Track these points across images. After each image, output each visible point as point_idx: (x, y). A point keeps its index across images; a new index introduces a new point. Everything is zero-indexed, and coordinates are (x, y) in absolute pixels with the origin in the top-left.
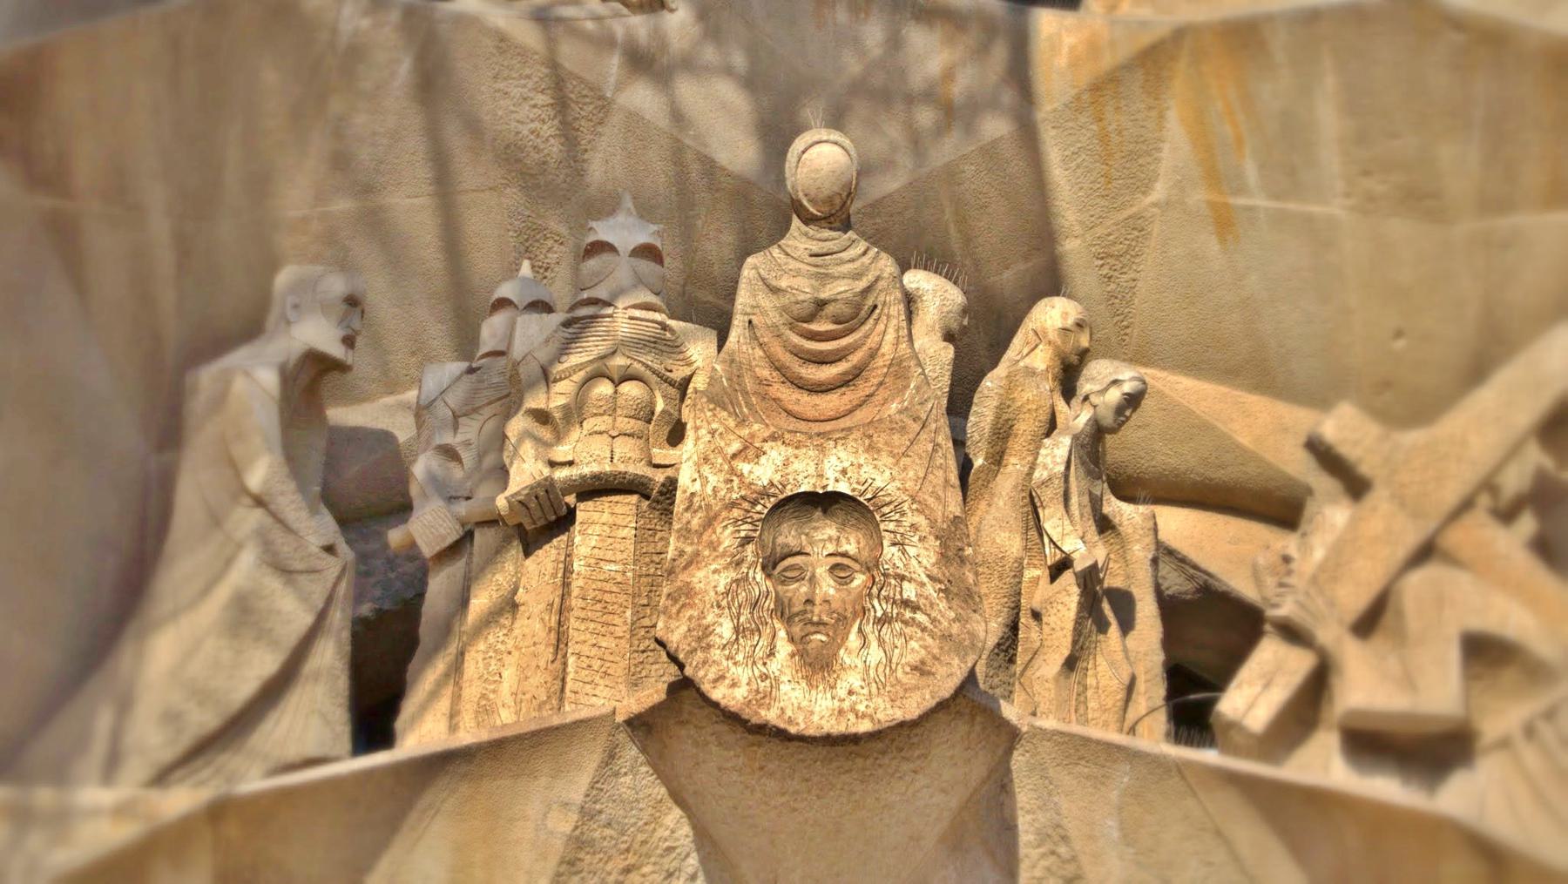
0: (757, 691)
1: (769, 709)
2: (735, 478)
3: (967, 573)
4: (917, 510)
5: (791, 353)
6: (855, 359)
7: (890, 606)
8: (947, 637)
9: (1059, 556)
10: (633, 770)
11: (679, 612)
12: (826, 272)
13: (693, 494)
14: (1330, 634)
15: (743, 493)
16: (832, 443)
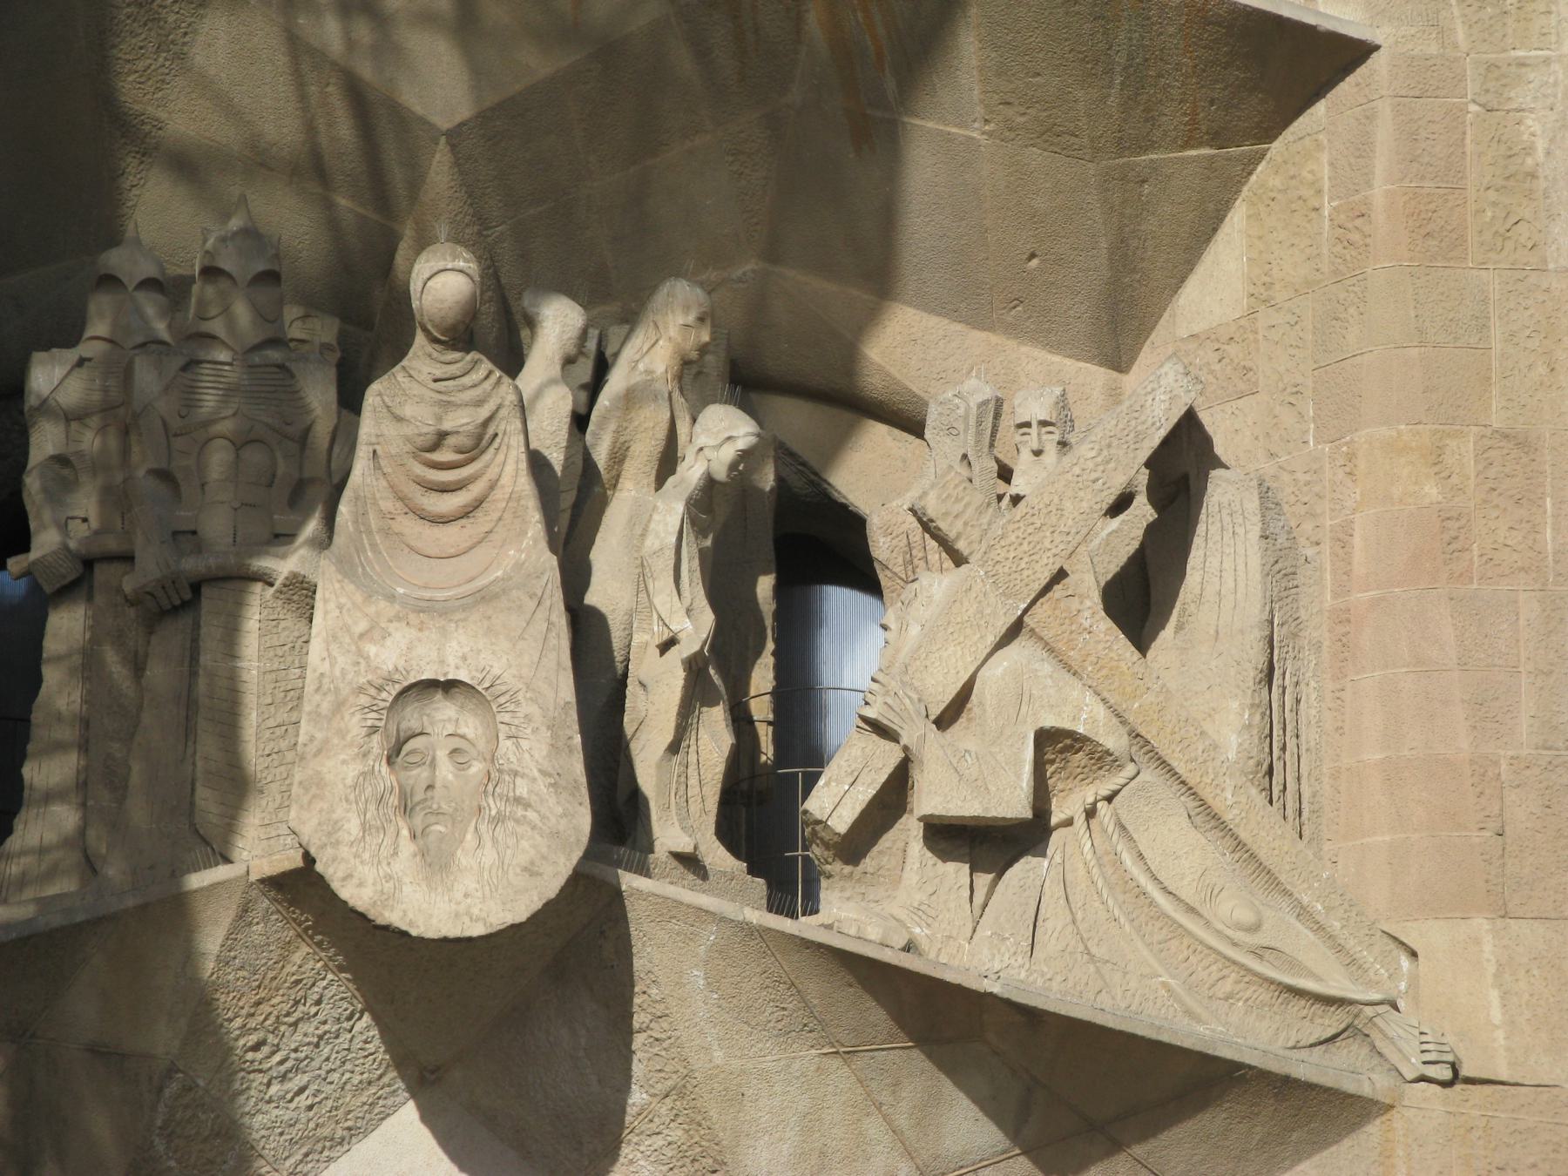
0: (382, 892)
1: (392, 911)
2: (361, 660)
3: (575, 763)
4: (531, 699)
5: (414, 482)
6: (476, 490)
7: (503, 804)
8: (555, 834)
9: (665, 637)
10: (265, 919)
11: (310, 802)
12: (449, 399)
13: (322, 674)
14: (915, 732)
15: (370, 677)
16: (453, 625)
